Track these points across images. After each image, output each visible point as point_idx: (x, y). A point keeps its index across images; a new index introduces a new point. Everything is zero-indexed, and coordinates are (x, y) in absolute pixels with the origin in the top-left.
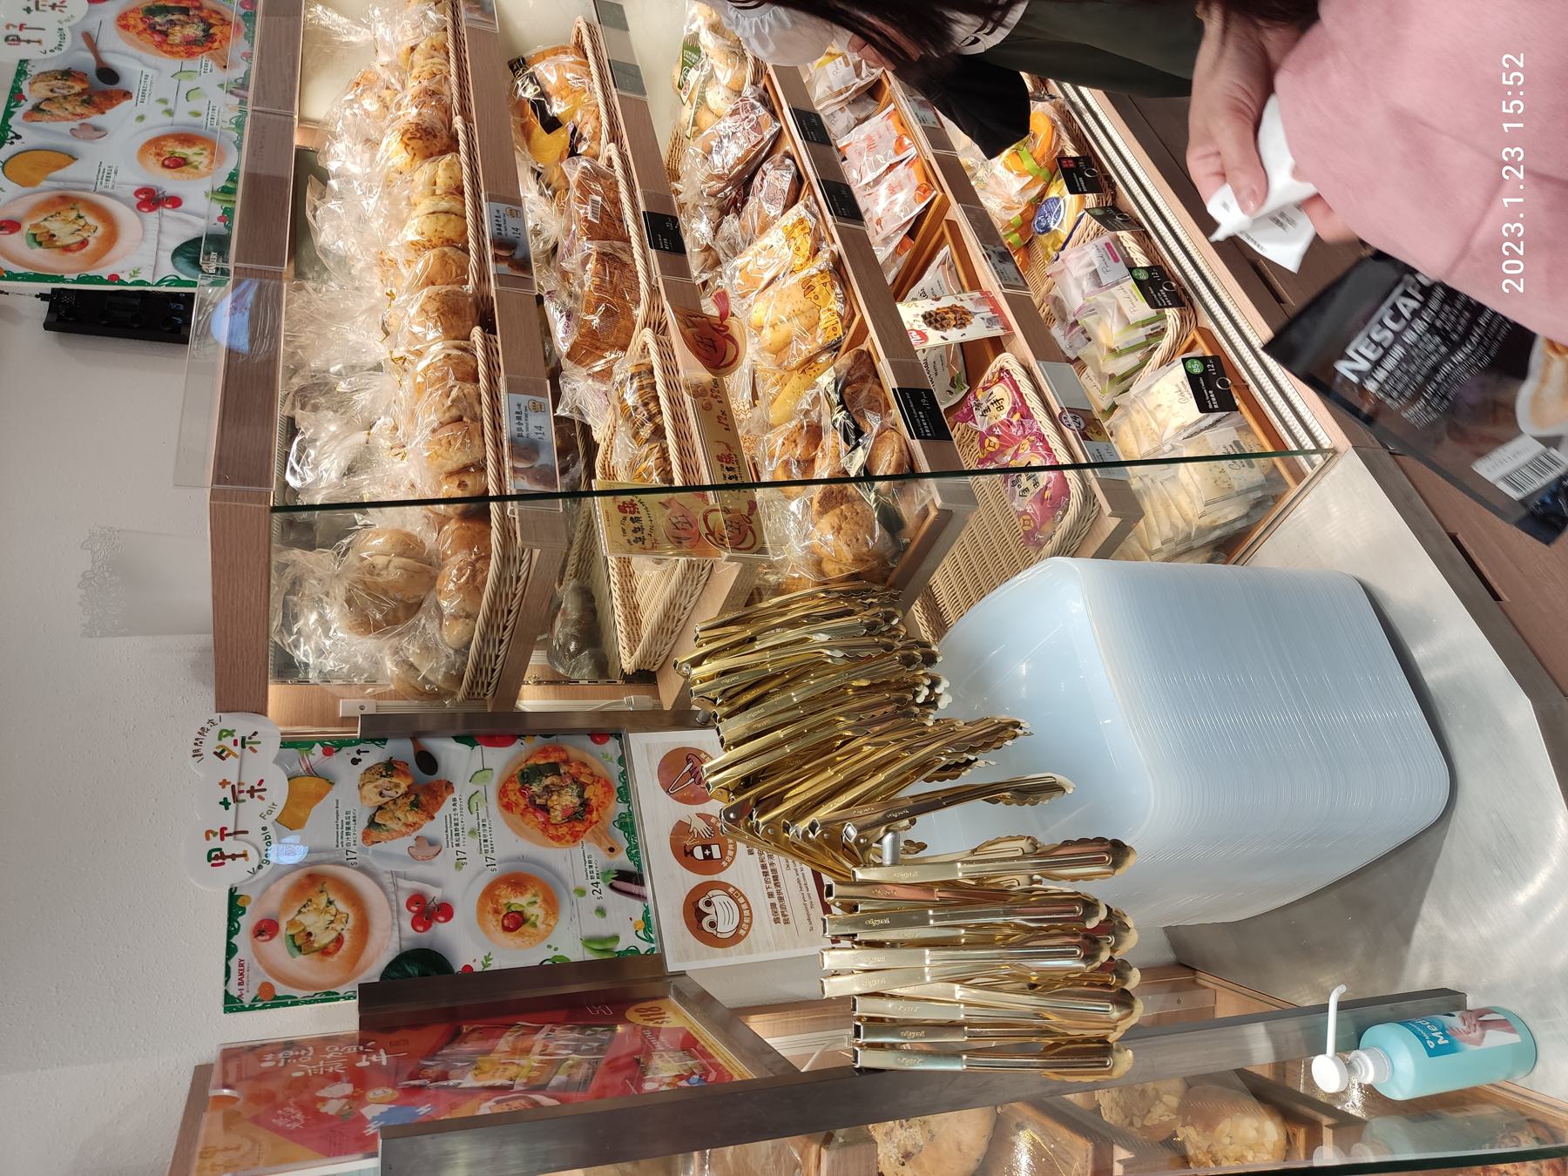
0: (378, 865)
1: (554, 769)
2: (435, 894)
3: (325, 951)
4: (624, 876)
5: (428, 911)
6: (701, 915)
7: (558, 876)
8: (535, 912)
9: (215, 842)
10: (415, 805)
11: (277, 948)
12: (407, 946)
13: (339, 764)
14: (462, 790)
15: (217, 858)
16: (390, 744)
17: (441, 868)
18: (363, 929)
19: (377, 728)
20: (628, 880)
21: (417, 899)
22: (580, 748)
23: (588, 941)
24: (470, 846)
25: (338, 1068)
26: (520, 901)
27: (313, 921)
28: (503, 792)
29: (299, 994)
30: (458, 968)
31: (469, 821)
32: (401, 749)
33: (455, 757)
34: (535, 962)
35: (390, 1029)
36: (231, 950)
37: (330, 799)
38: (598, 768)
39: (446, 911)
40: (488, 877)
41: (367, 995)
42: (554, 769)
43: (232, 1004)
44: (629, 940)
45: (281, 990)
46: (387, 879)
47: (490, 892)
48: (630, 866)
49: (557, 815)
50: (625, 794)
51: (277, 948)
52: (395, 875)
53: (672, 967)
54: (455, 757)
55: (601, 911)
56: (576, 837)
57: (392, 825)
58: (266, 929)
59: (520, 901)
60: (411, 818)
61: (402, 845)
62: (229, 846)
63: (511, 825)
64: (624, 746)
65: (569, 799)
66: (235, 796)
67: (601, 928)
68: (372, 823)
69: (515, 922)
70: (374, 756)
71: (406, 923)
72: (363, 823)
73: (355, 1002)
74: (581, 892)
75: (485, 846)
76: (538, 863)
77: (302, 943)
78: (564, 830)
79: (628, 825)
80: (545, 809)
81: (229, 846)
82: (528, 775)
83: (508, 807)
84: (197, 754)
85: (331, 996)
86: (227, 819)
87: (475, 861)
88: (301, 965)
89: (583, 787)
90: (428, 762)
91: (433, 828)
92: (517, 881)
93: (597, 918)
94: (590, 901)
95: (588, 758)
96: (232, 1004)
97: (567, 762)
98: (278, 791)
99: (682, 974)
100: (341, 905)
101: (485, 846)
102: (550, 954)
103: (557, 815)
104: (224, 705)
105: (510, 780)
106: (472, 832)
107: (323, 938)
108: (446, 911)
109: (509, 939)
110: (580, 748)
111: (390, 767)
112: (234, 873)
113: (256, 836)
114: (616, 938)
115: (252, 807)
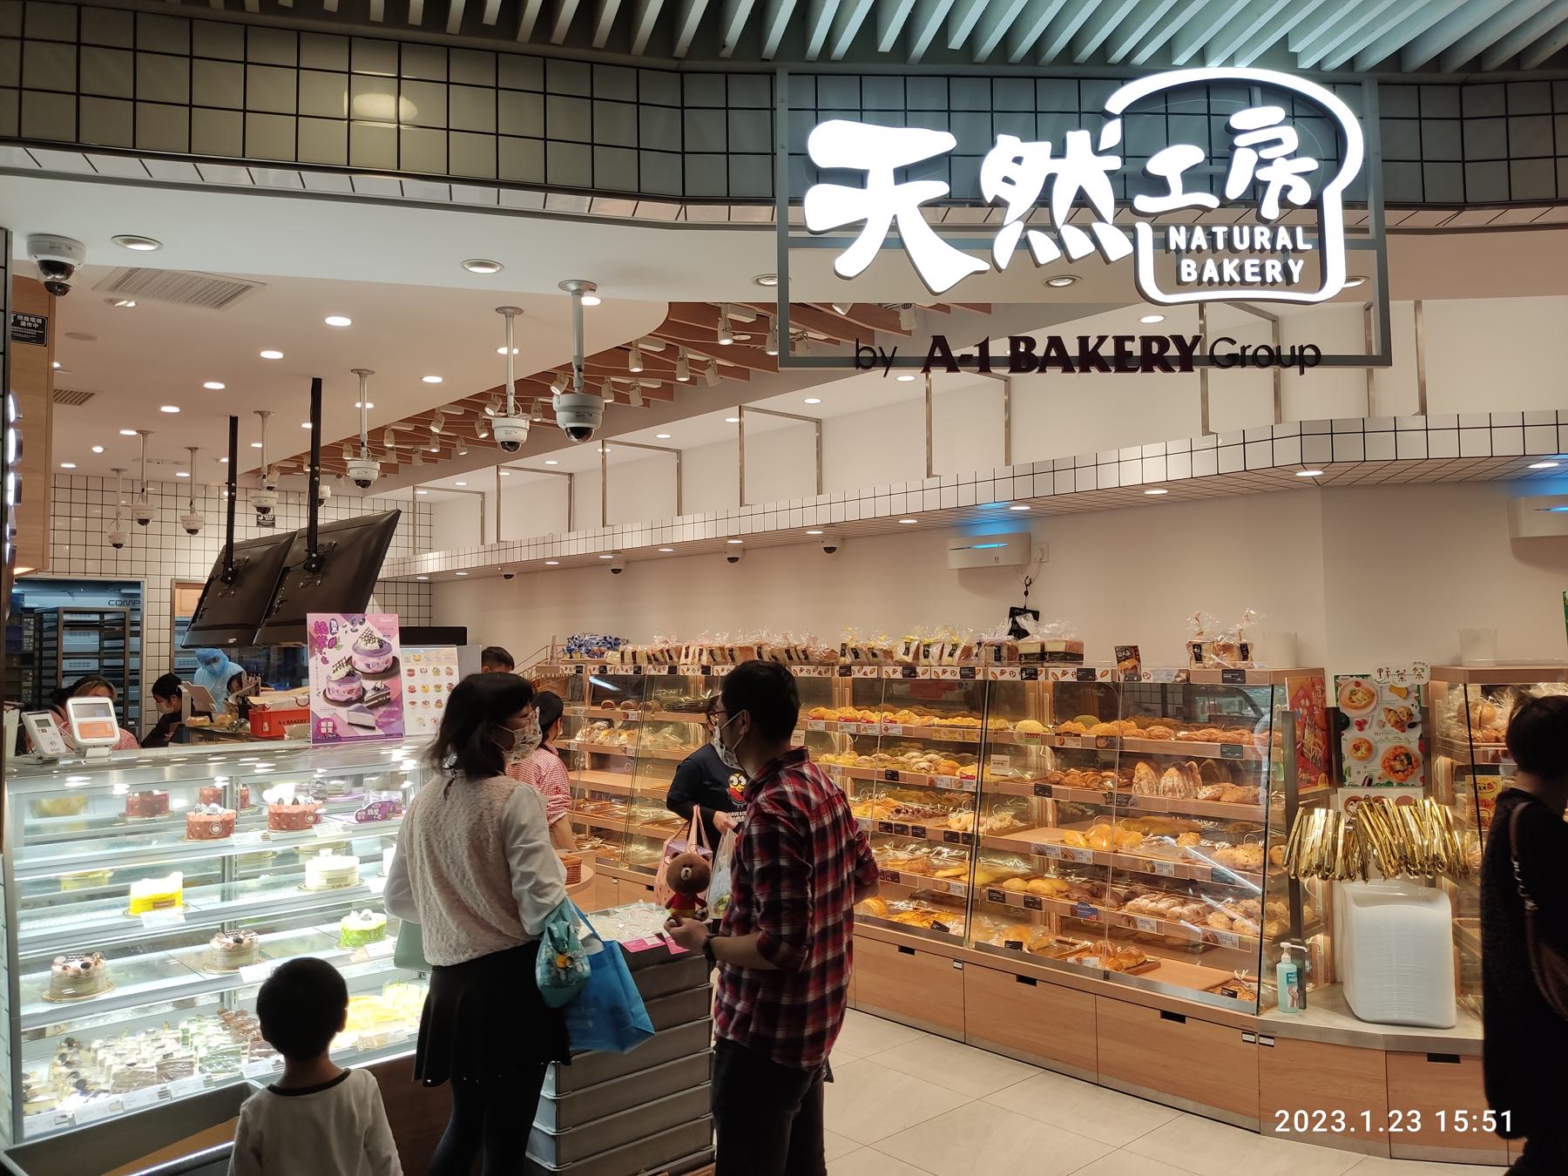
0: (1376, 713)
1: (1410, 763)
2: (1367, 726)
3: (1350, 698)
4: (1371, 781)
5: (1361, 725)
6: (1355, 801)
7: (1372, 761)
8: (1359, 754)
9: (1385, 670)
10: (1397, 722)
11: (1353, 687)
12: (1351, 719)
13: (1411, 701)
14: (1402, 735)
15: (1380, 671)
16: (1419, 715)
17: (1375, 728)
18: (1356, 708)
19: (1425, 712)
20: (1369, 782)
21: (1365, 722)
22: (1419, 772)
23: (1349, 768)
24: (1383, 737)
25: (1314, 702)
26: (1363, 750)
27: (1359, 695)
28: (1401, 747)
29: (1338, 693)
30: (1343, 732)
31: (1391, 737)
32: (1418, 718)
33: (1417, 732)
34: (1343, 752)
35: (1326, 714)
36: (1352, 676)
37: (1399, 698)
38: (1410, 777)
39: (1361, 729)
40: (1370, 740)
41: (1336, 710)
42: (1410, 763)
43: (1337, 677)
44: (1349, 780)
45: (1340, 689)
46: (1372, 714)
47: (1366, 741)
48: (1374, 783)
49: (1392, 763)
50: (1400, 785)
51: (1353, 687)
52: (1373, 717)
53: (1339, 790)
54: (1417, 732)
55: (1359, 773)
56: (1385, 768)
57: (1390, 716)
58: (1358, 684)
59: (1363, 750)
60: (1392, 721)
61: (1383, 717)
62: (1384, 674)
63: (1389, 749)
64: (1419, 787)
65: (1398, 766)
66: (1401, 675)
67: (1353, 772)
68: (1390, 710)
69: (1357, 748)
70: (1415, 711)
71: (1357, 719)
72: (1391, 708)
73: (1335, 706)
74: (1365, 767)
75: (1381, 741)
76: (1376, 756)
77: (1353, 693)
78: (1387, 764)
79: (1389, 784)
80: (1395, 759)
81: (1384, 674)
82: (1408, 756)
83: (1396, 748)
84: (1415, 663)
85: (1337, 701)
86: (1393, 672)
87: (1377, 738)
88: (1347, 693)
89: (1403, 772)
90: (1412, 725)
91: (1388, 726)
92: (1370, 749)
93: (1356, 771)
94: (1362, 770)
95: (1414, 775)
96: (1337, 677)
97: (1413, 768)
98: (1402, 685)
99: (1337, 792)
100: (1364, 702)
101: (1381, 741)
102: (1346, 757)
103: (1392, 763)
104: (1432, 669)
105: (1406, 750)
106: (1387, 738)
107: (1354, 698)
108: (1361, 729)
109: (1351, 746)
110: (1419, 772)
111: (1411, 715)
112: (1375, 676)
113: (1387, 680)
114: (1350, 776)
115: (1397, 678)
